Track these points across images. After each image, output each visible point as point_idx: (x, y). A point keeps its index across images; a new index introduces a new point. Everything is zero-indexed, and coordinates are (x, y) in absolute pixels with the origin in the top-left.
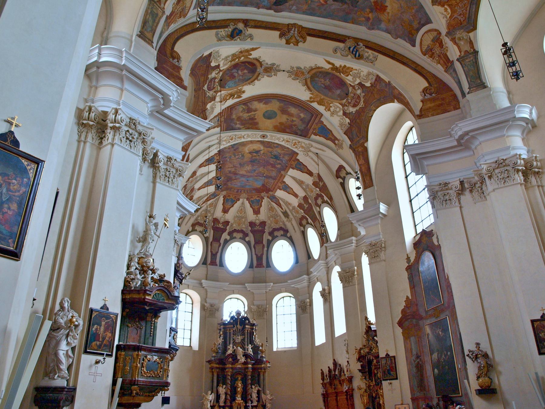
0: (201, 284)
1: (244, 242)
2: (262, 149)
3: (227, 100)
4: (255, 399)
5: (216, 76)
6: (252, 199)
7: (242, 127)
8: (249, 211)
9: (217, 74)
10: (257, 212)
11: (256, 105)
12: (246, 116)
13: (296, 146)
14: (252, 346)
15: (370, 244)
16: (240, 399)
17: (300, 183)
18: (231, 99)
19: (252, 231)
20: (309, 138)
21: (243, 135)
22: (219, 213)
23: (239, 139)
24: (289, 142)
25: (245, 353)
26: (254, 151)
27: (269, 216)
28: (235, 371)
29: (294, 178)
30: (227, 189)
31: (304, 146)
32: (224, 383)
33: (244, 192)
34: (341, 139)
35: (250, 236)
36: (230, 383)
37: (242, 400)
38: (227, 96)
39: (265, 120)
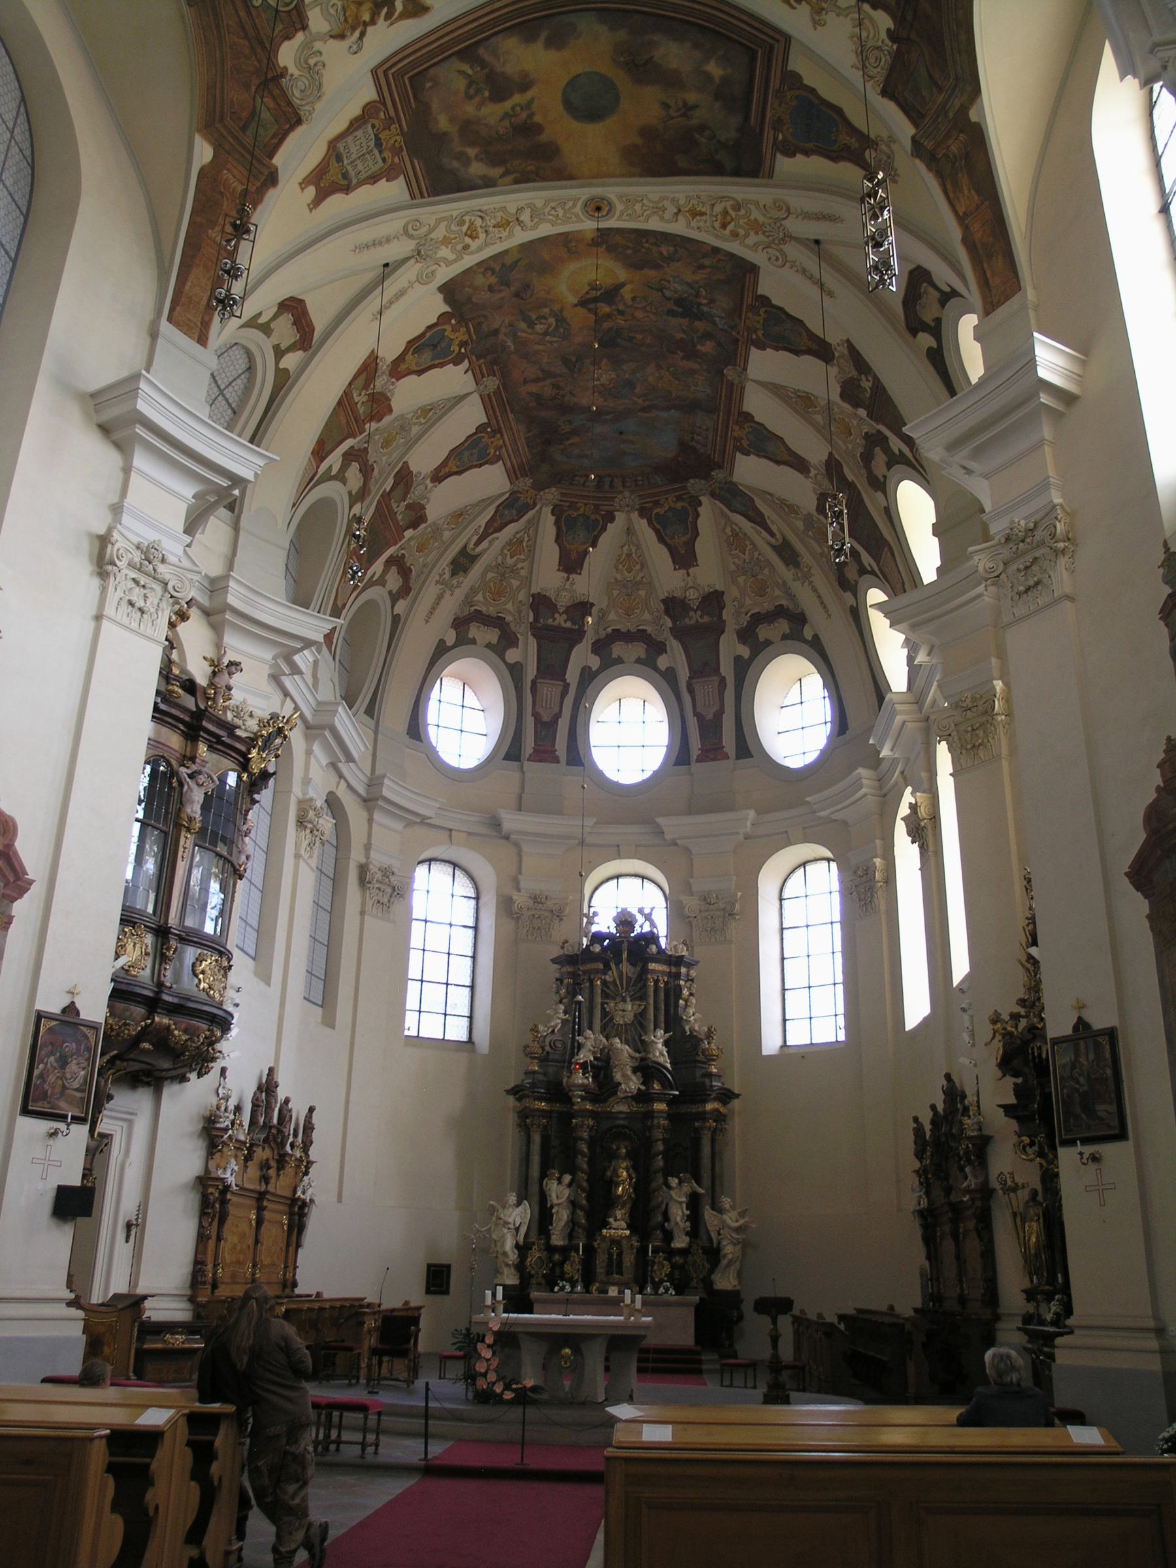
0: (495, 824)
1: (653, 672)
2: (622, 280)
3: (365, 24)
4: (682, 1225)
6: (658, 510)
7: (496, 172)
8: (658, 556)
10: (684, 558)
12: (492, 113)
13: (730, 227)
14: (667, 1035)
15: (1008, 539)
16: (624, 1225)
17: (802, 403)
18: (381, 21)
20: (770, 176)
21: (512, 209)
23: (504, 234)
24: (702, 214)
25: (643, 1059)
26: (593, 294)
27: (733, 568)
29: (776, 390)
30: (556, 479)
31: (761, 219)
32: (572, 1169)
33: (624, 486)
34: (885, 135)
35: (672, 648)
36: (585, 1166)
37: (629, 1227)
39: (575, 125)
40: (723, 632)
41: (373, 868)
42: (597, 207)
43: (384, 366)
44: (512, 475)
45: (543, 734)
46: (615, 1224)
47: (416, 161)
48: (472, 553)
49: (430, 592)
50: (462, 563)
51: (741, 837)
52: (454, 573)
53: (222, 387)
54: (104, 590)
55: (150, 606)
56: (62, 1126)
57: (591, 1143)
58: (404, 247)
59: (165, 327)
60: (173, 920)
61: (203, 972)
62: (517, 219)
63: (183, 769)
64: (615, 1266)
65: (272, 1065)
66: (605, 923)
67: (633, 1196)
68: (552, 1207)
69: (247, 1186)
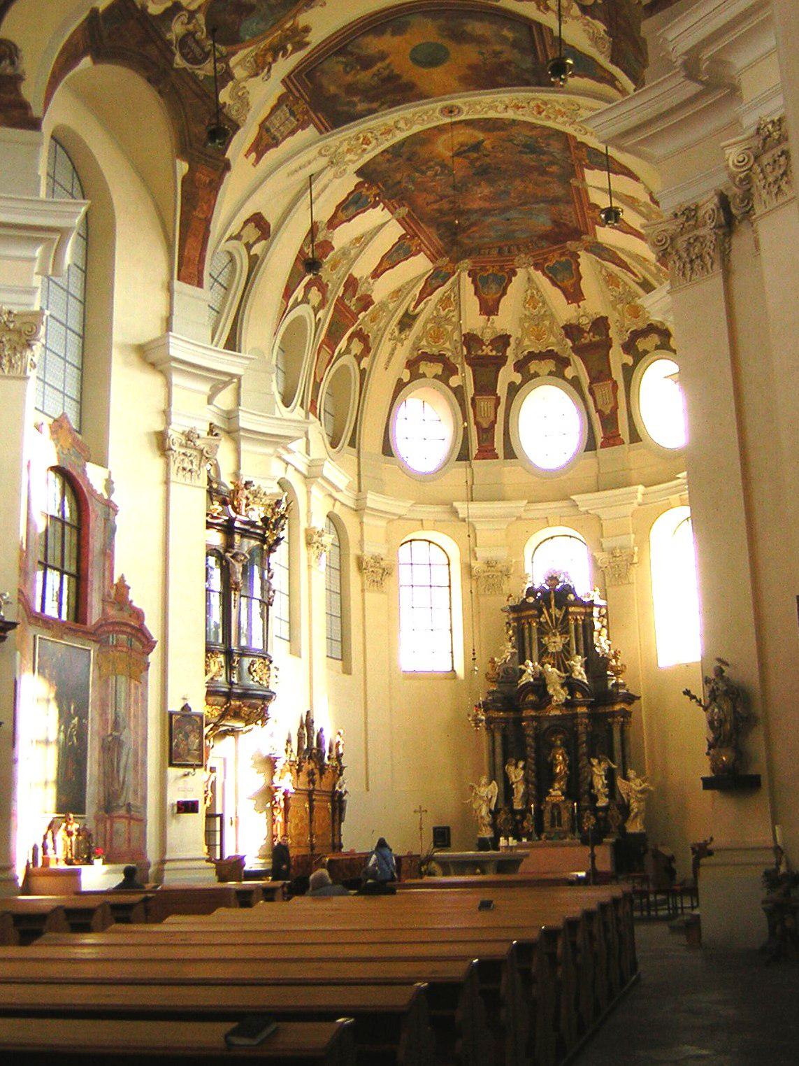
0: (455, 512)
3: (270, 64)
5: (190, 27)
7: (375, 105)
8: (554, 296)
9: (189, 23)
10: (574, 295)
11: (373, 44)
12: (364, 77)
13: (544, 113)
16: (560, 793)
19: (577, 350)
21: (391, 123)
22: (473, 319)
23: (389, 137)
26: (462, 149)
27: (612, 298)
28: (546, 725)
30: (467, 254)
33: (520, 251)
35: (575, 362)
38: (265, 55)
40: (611, 346)
41: (367, 558)
42: (450, 111)
43: (322, 226)
44: (432, 258)
45: (484, 436)
46: (554, 793)
47: (319, 115)
48: (412, 313)
49: (386, 347)
50: (407, 322)
51: (635, 505)
52: (401, 331)
53: (215, 277)
54: (167, 465)
55: (195, 468)
56: (191, 770)
57: (537, 737)
58: (323, 161)
59: (177, 284)
60: (234, 647)
61: (255, 671)
62: (396, 127)
63: (228, 555)
64: (557, 820)
65: (308, 709)
66: (538, 580)
67: (568, 772)
68: (513, 784)
69: (300, 787)
